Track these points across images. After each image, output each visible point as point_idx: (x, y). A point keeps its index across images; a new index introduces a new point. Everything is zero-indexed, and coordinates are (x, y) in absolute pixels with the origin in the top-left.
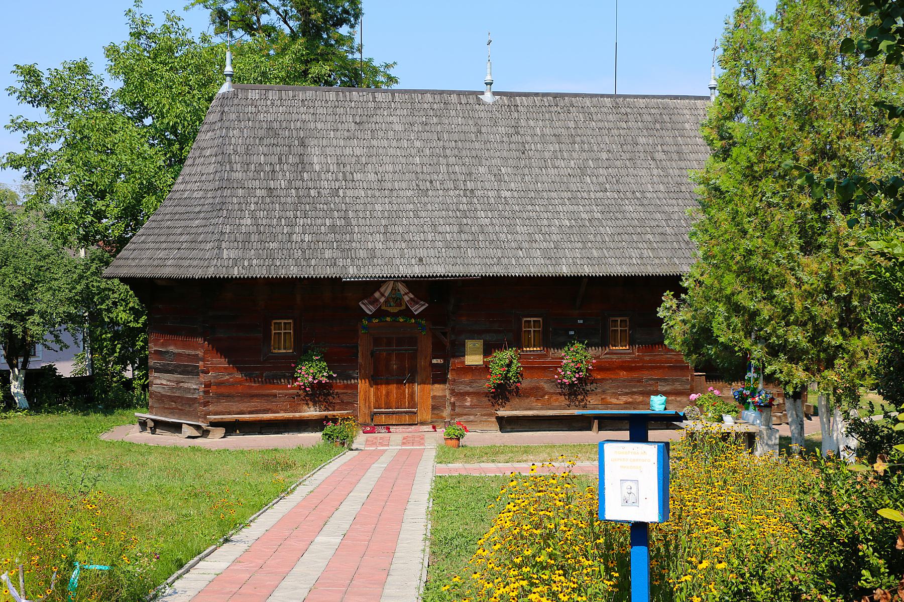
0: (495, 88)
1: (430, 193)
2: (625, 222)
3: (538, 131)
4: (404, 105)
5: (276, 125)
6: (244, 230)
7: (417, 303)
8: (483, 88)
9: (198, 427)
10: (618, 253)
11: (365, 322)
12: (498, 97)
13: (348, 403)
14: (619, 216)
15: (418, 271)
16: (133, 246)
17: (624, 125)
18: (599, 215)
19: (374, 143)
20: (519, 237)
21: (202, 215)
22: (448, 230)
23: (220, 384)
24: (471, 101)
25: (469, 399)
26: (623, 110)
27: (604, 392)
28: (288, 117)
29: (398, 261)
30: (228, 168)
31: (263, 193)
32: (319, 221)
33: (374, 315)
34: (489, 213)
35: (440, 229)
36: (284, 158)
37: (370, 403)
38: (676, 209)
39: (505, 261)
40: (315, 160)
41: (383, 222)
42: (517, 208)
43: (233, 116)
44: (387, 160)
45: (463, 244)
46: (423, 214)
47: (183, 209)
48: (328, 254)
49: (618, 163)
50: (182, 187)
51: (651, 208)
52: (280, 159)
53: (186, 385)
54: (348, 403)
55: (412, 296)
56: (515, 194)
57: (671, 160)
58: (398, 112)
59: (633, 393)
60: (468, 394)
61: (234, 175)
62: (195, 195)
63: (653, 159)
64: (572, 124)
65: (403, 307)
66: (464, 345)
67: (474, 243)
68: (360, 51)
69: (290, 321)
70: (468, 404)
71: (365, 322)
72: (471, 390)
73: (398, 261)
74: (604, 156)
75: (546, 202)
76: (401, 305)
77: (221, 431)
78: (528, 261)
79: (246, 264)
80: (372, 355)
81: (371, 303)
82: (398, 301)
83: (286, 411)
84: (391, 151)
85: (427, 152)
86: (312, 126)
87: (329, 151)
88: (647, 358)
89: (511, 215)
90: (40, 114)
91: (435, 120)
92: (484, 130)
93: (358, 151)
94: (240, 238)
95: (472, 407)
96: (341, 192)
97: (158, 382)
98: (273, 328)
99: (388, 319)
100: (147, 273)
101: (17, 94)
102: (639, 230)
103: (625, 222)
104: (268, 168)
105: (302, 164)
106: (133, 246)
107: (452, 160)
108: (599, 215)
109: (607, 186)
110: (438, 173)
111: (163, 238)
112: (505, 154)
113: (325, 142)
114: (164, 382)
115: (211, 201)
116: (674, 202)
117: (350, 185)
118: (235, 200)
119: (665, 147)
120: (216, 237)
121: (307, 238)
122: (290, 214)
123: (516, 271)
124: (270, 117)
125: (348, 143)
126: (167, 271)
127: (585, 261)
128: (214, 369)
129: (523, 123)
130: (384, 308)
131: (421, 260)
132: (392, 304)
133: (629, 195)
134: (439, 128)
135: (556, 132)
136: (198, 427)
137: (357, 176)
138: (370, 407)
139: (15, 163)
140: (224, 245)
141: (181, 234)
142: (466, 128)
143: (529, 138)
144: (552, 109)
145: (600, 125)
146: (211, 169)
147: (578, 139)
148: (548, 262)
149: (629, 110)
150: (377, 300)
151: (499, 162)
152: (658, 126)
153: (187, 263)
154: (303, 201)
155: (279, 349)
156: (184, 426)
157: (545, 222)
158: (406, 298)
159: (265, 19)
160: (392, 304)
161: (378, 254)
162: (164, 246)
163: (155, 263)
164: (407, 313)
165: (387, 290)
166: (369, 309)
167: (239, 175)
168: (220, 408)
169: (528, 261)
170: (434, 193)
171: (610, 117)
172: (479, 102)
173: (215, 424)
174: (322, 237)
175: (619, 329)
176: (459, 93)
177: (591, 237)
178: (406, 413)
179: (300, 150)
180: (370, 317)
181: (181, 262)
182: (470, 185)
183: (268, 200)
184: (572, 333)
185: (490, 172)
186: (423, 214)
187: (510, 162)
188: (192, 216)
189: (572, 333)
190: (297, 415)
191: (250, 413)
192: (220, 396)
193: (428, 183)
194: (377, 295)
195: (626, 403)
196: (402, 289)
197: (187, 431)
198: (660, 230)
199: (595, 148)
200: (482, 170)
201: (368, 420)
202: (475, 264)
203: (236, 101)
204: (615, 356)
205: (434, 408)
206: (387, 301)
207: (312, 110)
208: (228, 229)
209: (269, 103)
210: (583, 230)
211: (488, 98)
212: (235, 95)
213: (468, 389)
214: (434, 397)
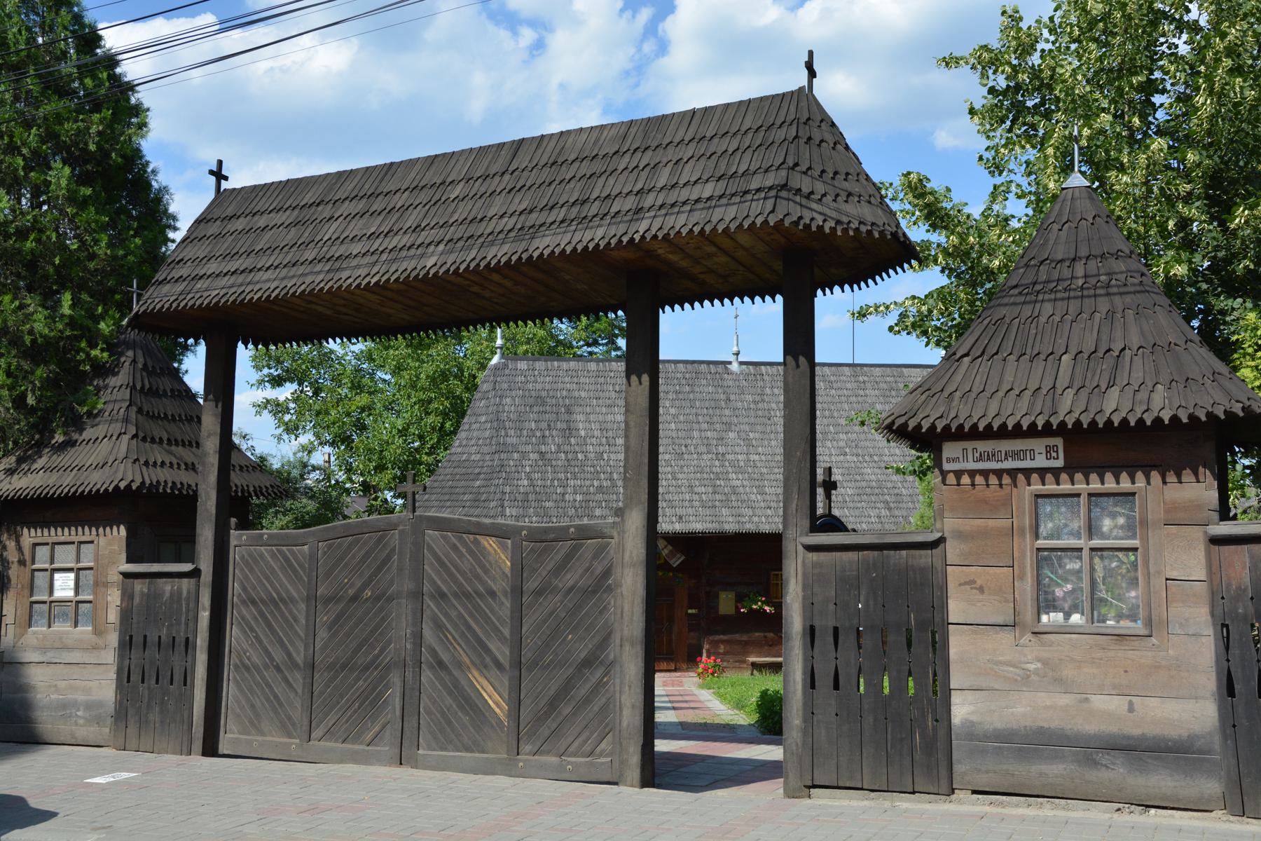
0: (741, 359)
1: (686, 456)
2: (864, 484)
5: (544, 394)
6: (522, 490)
8: (732, 358)
10: (857, 512)
14: (858, 477)
17: (861, 392)
20: (768, 498)
21: (482, 476)
26: (861, 379)
28: (555, 386)
32: (588, 483)
35: (696, 490)
39: (756, 519)
40: (581, 426)
42: (765, 470)
43: (505, 386)
46: (680, 476)
50: (459, 450)
56: (763, 458)
60: (722, 642)
61: (509, 440)
62: (473, 457)
66: (718, 596)
67: (726, 502)
85: (681, 418)
86: (576, 394)
91: (687, 388)
92: (732, 397)
94: (519, 497)
95: (725, 654)
96: (605, 456)
102: (877, 491)
103: (864, 484)
105: (569, 431)
110: (692, 438)
111: (447, 497)
112: (752, 420)
113: (588, 409)
117: (613, 449)
118: (512, 463)
120: (498, 496)
121: (579, 498)
122: (562, 476)
124: (539, 386)
125: (609, 410)
129: (768, 391)
131: (681, 518)
134: (691, 396)
140: (506, 504)
141: (464, 494)
143: (774, 406)
145: (840, 392)
146: (487, 434)
151: (747, 428)
152: (893, 393)
154: (573, 463)
167: (514, 440)
171: (849, 386)
172: (729, 372)
176: (709, 363)
179: (566, 417)
183: (540, 463)
185: (739, 437)
186: (680, 476)
187: (759, 428)
198: (896, 491)
200: (731, 435)
203: (507, 372)
208: (508, 489)
211: (735, 367)
212: (506, 366)
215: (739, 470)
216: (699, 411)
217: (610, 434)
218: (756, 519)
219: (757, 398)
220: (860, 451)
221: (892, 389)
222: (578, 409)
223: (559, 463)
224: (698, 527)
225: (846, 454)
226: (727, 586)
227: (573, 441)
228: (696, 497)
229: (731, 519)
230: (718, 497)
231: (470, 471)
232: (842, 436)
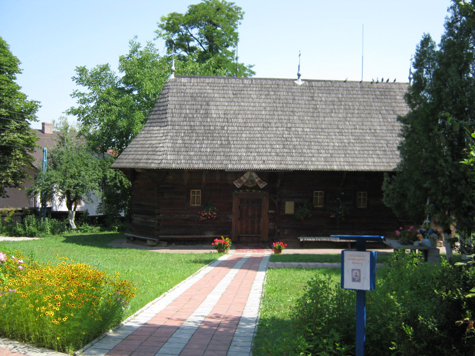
1: (269, 128)
3: (324, 99)
4: (257, 86)
5: (195, 95)
7: (261, 183)
9: (154, 241)
10: (362, 160)
11: (236, 192)
12: (304, 82)
15: (262, 167)
16: (125, 153)
18: (353, 141)
19: (242, 104)
20: (313, 151)
22: (278, 147)
24: (290, 84)
25: (286, 231)
28: (201, 91)
29: (253, 162)
30: (171, 115)
31: (189, 128)
32: (215, 142)
33: (241, 188)
34: (298, 139)
35: (274, 146)
36: (198, 111)
38: (392, 138)
39: (306, 163)
40: (213, 112)
41: (246, 143)
42: (312, 137)
43: (175, 91)
44: (249, 112)
45: (285, 154)
47: (149, 135)
48: (218, 158)
49: (362, 115)
51: (379, 138)
52: (196, 111)
53: (149, 221)
55: (259, 179)
56: (312, 130)
57: (390, 114)
58: (254, 89)
61: (174, 119)
63: (380, 113)
64: (340, 96)
65: (255, 185)
66: (284, 204)
67: (290, 154)
68: (237, 59)
69: (200, 190)
71: (236, 192)
73: (253, 162)
74: (356, 112)
75: (327, 134)
77: (165, 243)
78: (317, 163)
79: (179, 162)
80: (239, 207)
81: (239, 182)
82: (253, 181)
83: (197, 234)
84: (250, 108)
86: (212, 95)
87: (220, 108)
89: (309, 140)
90: (85, 90)
91: (272, 93)
92: (296, 98)
93: (234, 108)
94: (176, 149)
96: (226, 128)
97: (136, 218)
98: (191, 193)
99: (248, 190)
100: (132, 165)
101: (76, 80)
104: (191, 116)
105: (207, 114)
106: (125, 153)
107: (280, 113)
108: (353, 141)
109: (357, 126)
110: (273, 119)
111: (139, 149)
113: (218, 103)
114: (139, 219)
115: (163, 131)
116: (391, 135)
117: (230, 124)
119: (386, 108)
121: (208, 150)
122: (201, 138)
123: (311, 168)
124: (191, 91)
126: (141, 165)
127: (345, 163)
129: (316, 95)
130: (245, 185)
131: (264, 161)
133: (368, 131)
135: (332, 99)
136: (154, 241)
137: (233, 120)
139: (74, 112)
142: (288, 97)
143: (319, 102)
144: (330, 88)
145: (355, 96)
147: (343, 103)
148: (327, 163)
149: (368, 89)
152: (383, 97)
153: (150, 161)
155: (194, 204)
156: (148, 240)
157: (326, 144)
158: (257, 180)
159: (192, 44)
160: (250, 183)
161: (243, 158)
162: (140, 153)
163: (136, 161)
164: (257, 187)
165: (247, 176)
166: (238, 185)
169: (317, 163)
170: (271, 129)
172: (295, 85)
174: (216, 150)
175: (362, 197)
177: (349, 152)
179: (207, 107)
180: (238, 189)
181: (147, 161)
182: (289, 125)
188: (153, 139)
190: (202, 236)
193: (268, 124)
194: (242, 178)
196: (255, 175)
197: (149, 242)
198: (383, 149)
199: (352, 107)
200: (295, 118)
202: (291, 164)
203: (176, 84)
206: (247, 182)
207: (212, 88)
209: (192, 84)
210: (345, 148)
215: (298, 136)
216: (278, 105)
217: (229, 116)
218: (306, 163)
219: (310, 99)
220: (364, 127)
221: (381, 95)
222: (212, 103)
223: (200, 131)
224: (274, 167)
225: (356, 129)
226: (290, 198)
227: (209, 120)
228: (273, 150)
229: (292, 163)
230: (285, 150)
231: (152, 135)
232: (355, 119)
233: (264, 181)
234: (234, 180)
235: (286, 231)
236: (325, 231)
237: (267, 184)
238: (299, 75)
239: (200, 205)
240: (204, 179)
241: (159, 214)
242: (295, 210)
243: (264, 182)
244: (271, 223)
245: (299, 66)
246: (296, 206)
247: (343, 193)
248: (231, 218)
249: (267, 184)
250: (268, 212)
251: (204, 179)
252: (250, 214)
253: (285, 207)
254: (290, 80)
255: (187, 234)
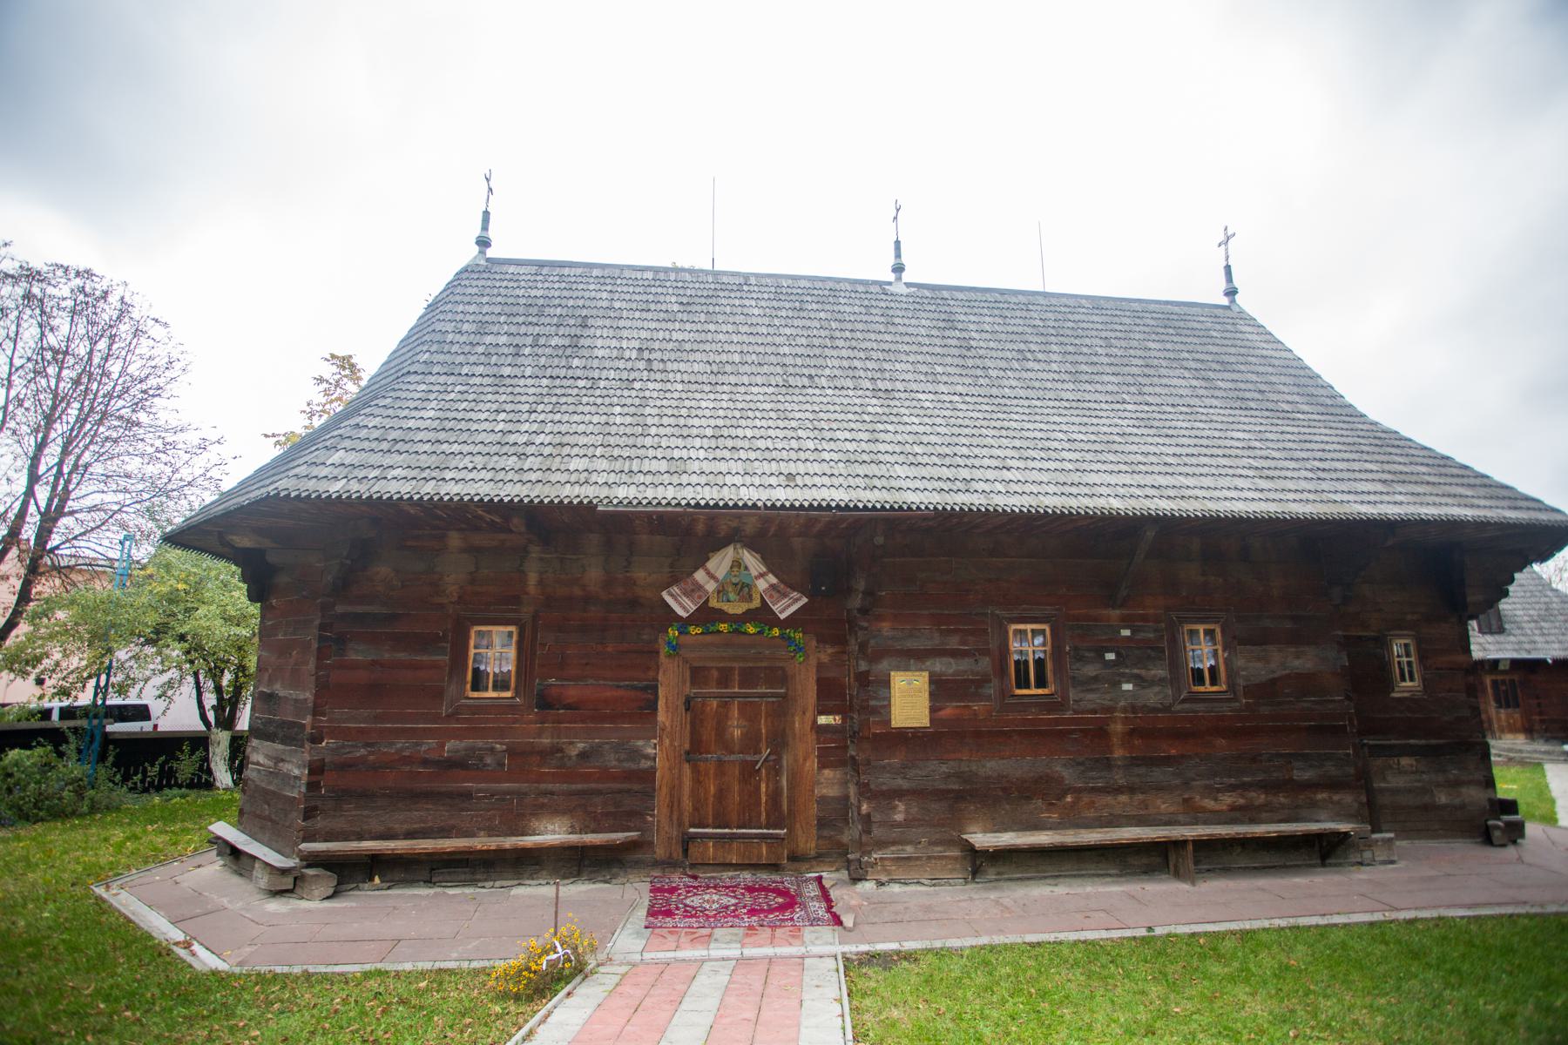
7: (785, 595)
11: (673, 633)
13: (632, 814)
23: (345, 766)
25: (901, 807)
27: (1186, 784)
33: (693, 619)
37: (681, 814)
54: (632, 814)
55: (773, 579)
59: (1245, 787)
60: (899, 794)
65: (756, 603)
66: (887, 684)
69: (512, 628)
70: (899, 817)
72: (905, 785)
76: (750, 598)
80: (688, 704)
82: (745, 590)
83: (492, 832)
88: (1265, 710)
95: (907, 823)
99: (723, 627)
128: (335, 732)
130: (713, 603)
132: (732, 596)
138: (680, 824)
150: (700, 587)
158: (762, 585)
160: (732, 596)
164: (763, 615)
166: (682, 606)
168: (339, 824)
173: (313, 860)
178: (763, 837)
180: (684, 624)
184: (1111, 656)
189: (1111, 656)
191: (410, 835)
192: (342, 796)
194: (700, 575)
195: (1233, 808)
201: (678, 853)
204: (1200, 707)
205: (822, 823)
206: (721, 591)
213: (901, 783)
214: (823, 800)
224: (839, 496)
226: (911, 658)
233: (794, 589)
234: (667, 586)
235: (901, 807)
236: (1069, 799)
237: (805, 600)
238: (898, 269)
239: (508, 694)
240: (533, 578)
241: (315, 739)
242: (933, 710)
243: (795, 594)
244: (826, 772)
245: (897, 243)
246: (940, 690)
247: (1126, 633)
248: (650, 751)
249: (805, 600)
250: (815, 721)
251: (533, 578)
252: (737, 733)
253: (889, 699)
254: (875, 283)
255: (444, 832)
